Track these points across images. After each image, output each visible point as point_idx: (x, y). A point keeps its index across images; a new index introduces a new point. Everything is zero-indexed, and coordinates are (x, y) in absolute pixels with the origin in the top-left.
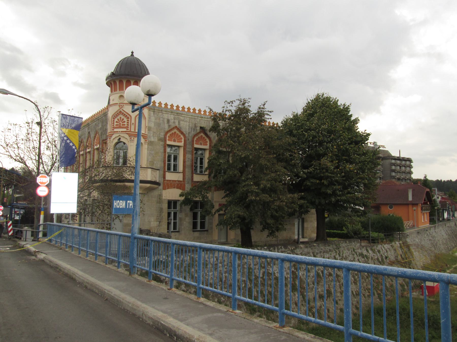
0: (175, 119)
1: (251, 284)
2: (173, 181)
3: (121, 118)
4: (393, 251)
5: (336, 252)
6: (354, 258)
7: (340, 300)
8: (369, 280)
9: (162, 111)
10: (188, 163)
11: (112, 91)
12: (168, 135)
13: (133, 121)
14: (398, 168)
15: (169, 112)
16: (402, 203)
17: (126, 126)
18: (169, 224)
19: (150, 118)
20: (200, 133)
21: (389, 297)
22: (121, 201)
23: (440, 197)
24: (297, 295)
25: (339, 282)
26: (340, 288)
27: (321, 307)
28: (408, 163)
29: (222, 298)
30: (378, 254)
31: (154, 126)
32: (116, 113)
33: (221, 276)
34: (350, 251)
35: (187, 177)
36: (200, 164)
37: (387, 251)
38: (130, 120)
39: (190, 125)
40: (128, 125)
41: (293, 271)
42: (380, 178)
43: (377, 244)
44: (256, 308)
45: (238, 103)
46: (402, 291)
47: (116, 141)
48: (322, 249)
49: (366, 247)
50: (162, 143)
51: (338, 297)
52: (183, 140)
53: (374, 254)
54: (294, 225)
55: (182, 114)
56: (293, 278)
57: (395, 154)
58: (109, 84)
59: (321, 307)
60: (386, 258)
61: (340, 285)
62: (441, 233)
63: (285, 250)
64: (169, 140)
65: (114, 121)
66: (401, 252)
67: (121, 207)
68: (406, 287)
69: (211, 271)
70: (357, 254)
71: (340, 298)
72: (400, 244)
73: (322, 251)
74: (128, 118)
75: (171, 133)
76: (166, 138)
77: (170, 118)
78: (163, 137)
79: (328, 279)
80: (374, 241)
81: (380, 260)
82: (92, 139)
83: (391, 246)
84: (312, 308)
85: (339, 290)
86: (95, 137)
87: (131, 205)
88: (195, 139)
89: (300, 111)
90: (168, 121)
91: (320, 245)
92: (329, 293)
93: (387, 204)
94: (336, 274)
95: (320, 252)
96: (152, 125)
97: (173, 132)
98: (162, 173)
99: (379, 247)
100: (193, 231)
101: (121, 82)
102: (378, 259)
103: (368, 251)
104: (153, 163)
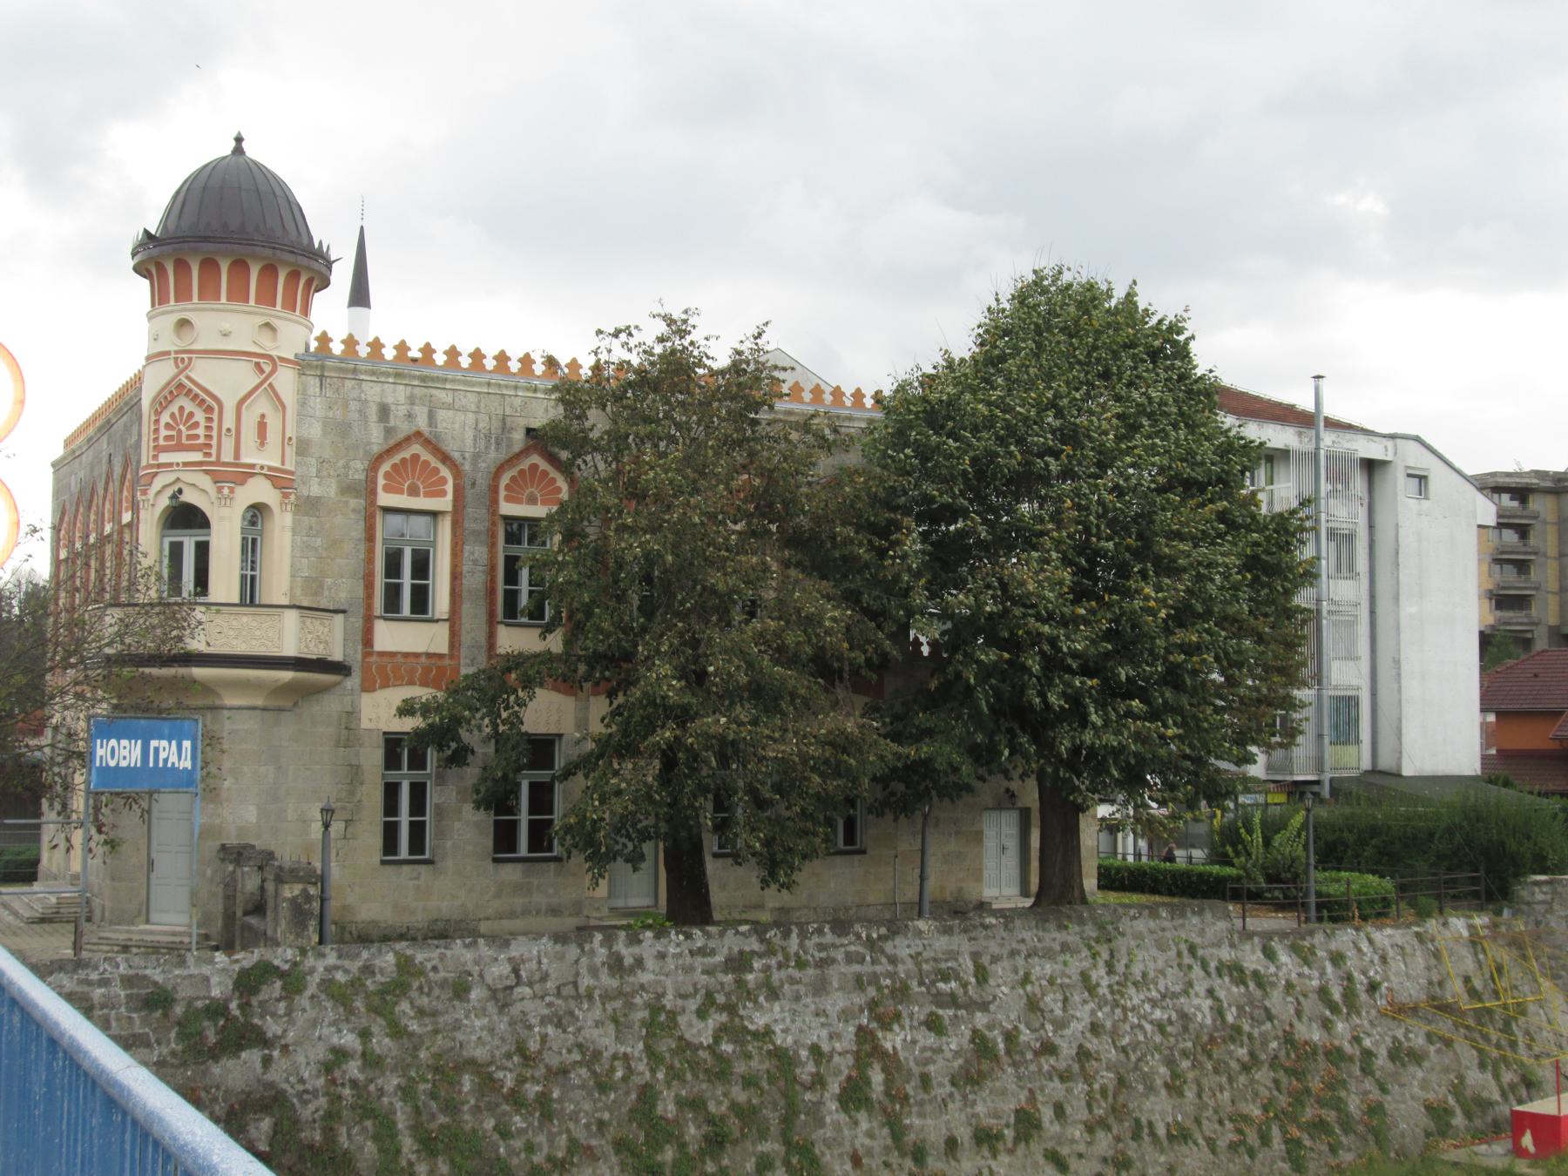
0: (412, 400)
1: (653, 1071)
2: (406, 655)
3: (182, 409)
4: (1420, 961)
5: (1094, 956)
6: (1190, 984)
7: (1080, 1156)
8: (1252, 1081)
9: (355, 371)
10: (474, 580)
11: (153, 305)
12: (386, 467)
13: (229, 422)
15: (389, 375)
17: (202, 440)
18: (390, 832)
22: (124, 742)
24: (864, 1126)
26: (1089, 1106)
29: (518, 1118)
30: (1329, 969)
31: (325, 433)
32: (166, 392)
33: (524, 1033)
34: (1172, 953)
35: (466, 639)
36: (507, 582)
37: (1384, 959)
38: (215, 416)
39: (481, 426)
41: (860, 1028)
43: (1328, 926)
44: (660, 1165)
45: (651, 333)
46: (1428, 1134)
47: (164, 502)
48: (1023, 941)
49: (1267, 936)
50: (357, 503)
51: (1073, 1141)
52: (449, 487)
53: (1306, 970)
54: (978, 837)
55: (445, 380)
56: (857, 1056)
60: (1373, 987)
63: (838, 941)
64: (387, 489)
65: (157, 421)
66: (1469, 965)
67: (124, 764)
68: (1459, 1120)
69: (483, 1012)
70: (1204, 966)
71: (1082, 1148)
72: (1471, 927)
73: (1023, 948)
74: (209, 409)
75: (396, 459)
76: (375, 482)
77: (390, 400)
78: (363, 477)
79: (1033, 1067)
80: (1333, 912)
81: (1336, 995)
82: (117, 483)
83: (1418, 935)
85: (1083, 1114)
86: (123, 476)
87: (163, 755)
88: (505, 480)
90: (384, 411)
91: (1018, 923)
92: (1027, 1124)
94: (1080, 1046)
95: (1013, 954)
97: (406, 454)
98: (358, 622)
99: (1345, 938)
100: (496, 860)
101: (182, 266)
102: (1323, 992)
103: (1269, 954)
104: (321, 586)
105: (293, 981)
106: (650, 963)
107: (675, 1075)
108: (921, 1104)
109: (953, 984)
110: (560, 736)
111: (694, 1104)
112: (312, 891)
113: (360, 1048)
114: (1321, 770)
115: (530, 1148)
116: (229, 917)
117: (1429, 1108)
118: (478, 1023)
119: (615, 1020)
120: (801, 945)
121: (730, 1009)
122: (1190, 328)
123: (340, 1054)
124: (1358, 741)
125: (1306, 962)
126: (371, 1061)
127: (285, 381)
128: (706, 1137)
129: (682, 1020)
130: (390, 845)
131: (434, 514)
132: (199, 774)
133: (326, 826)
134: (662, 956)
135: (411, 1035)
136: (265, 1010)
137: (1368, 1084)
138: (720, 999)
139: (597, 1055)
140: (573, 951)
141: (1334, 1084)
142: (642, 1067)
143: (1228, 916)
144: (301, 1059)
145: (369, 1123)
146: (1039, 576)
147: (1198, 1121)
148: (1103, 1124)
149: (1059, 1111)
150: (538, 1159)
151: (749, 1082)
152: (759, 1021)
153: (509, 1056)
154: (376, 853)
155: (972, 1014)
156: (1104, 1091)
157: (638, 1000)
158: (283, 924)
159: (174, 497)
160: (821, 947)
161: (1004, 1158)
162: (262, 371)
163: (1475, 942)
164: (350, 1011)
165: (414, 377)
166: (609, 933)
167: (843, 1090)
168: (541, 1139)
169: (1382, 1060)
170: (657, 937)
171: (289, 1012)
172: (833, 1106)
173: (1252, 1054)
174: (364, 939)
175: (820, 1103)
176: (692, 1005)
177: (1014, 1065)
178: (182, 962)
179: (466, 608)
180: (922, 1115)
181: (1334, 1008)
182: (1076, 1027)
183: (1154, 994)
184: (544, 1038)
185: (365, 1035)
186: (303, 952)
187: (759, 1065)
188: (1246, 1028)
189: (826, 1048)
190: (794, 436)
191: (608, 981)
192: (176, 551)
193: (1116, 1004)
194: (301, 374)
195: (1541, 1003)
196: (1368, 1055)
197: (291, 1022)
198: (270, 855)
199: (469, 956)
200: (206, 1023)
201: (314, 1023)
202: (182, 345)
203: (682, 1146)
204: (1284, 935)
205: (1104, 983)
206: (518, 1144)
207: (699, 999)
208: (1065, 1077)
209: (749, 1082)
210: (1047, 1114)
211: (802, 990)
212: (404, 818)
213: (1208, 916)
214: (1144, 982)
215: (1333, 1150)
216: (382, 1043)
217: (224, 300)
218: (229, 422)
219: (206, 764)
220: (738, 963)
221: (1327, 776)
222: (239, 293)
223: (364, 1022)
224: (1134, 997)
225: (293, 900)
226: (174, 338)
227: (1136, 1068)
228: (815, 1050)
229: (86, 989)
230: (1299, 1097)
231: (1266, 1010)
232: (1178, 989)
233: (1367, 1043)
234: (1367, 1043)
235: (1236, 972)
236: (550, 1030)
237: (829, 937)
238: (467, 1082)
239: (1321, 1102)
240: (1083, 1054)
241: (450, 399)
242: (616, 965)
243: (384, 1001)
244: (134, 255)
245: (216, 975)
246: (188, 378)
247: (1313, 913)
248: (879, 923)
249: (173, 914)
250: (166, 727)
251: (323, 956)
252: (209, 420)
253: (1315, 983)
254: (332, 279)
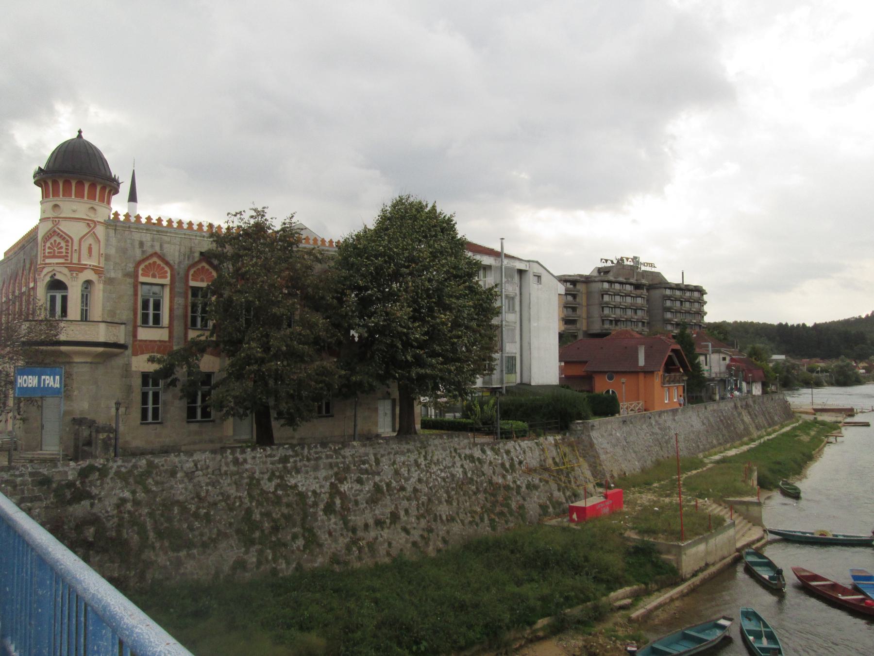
0: (153, 240)
1: (251, 503)
2: (151, 341)
5: (420, 453)
6: (455, 463)
7: (414, 528)
8: (477, 498)
10: (179, 312)
12: (142, 266)
13: (76, 247)
14: (678, 304)
15: (142, 229)
16: (628, 370)
17: (64, 254)
20: (199, 261)
21: (512, 525)
22: (30, 377)
23: (728, 358)
24: (333, 520)
25: (417, 500)
26: (418, 510)
27: (376, 538)
28: (696, 294)
30: (505, 456)
34: (448, 452)
35: (175, 334)
37: (524, 452)
39: (182, 250)
41: (332, 484)
42: (643, 323)
46: (540, 515)
47: (48, 279)
49: (483, 445)
50: (131, 281)
52: (169, 275)
54: (376, 410)
56: (330, 494)
57: (673, 278)
59: (376, 538)
60: (520, 463)
61: (418, 505)
62: (693, 421)
64: (143, 275)
66: (554, 453)
67: (30, 386)
68: (551, 510)
69: (182, 482)
70: (460, 456)
71: (415, 525)
72: (555, 440)
74: (67, 241)
77: (144, 240)
80: (507, 435)
81: (508, 466)
84: (359, 539)
85: (416, 513)
86: (30, 268)
87: (47, 382)
88: (192, 272)
89: (372, 226)
90: (141, 244)
92: (395, 517)
93: (605, 372)
95: (389, 453)
96: (112, 251)
97: (151, 261)
98: (130, 328)
99: (510, 445)
100: (188, 422)
101: (55, 183)
102: (503, 465)
103: (484, 451)
104: (115, 313)
105: (103, 472)
106: (249, 461)
107: (259, 504)
108: (355, 511)
109: (367, 466)
110: (213, 373)
111: (268, 514)
112: (111, 435)
113: (131, 498)
114: (502, 382)
115: (202, 535)
116: (76, 447)
117: (540, 506)
118: (180, 486)
119: (236, 483)
120: (309, 452)
121: (281, 477)
122: (455, 219)
123: (124, 501)
124: (516, 373)
125: (497, 454)
126: (136, 503)
127: (100, 231)
128: (272, 528)
129: (262, 482)
130: (144, 416)
131: (163, 286)
132: (63, 390)
133: (117, 409)
134: (254, 458)
135: (153, 491)
136: (92, 483)
137: (519, 498)
138: (277, 474)
139: (229, 497)
140: (219, 457)
141: (507, 498)
142: (247, 501)
143: (468, 438)
144: (107, 503)
145: (136, 528)
146: (401, 311)
147: (458, 514)
148: (423, 516)
149: (407, 511)
150: (205, 539)
151: (288, 505)
152: (293, 481)
153: (193, 499)
154: (139, 421)
155: (374, 476)
156: (423, 504)
157: (245, 475)
158: (99, 449)
159: (52, 277)
160: (316, 453)
161: (386, 531)
163: (556, 445)
164: (127, 483)
166: (233, 450)
167: (325, 507)
168: (206, 530)
169: (524, 489)
170: (252, 450)
171: (102, 484)
172: (321, 513)
173: (477, 488)
174: (134, 454)
175: (315, 513)
176: (266, 476)
177: (390, 495)
178: (56, 466)
179: (176, 323)
180: (355, 516)
181: (507, 471)
182: (413, 480)
183: (442, 467)
184: (207, 491)
185: (134, 492)
186: (108, 460)
187: (292, 498)
188: (475, 479)
189: (318, 491)
190: (306, 257)
191: (233, 468)
192: (53, 299)
193: (428, 471)
194: (107, 228)
195: (579, 467)
196: (519, 487)
197: (103, 489)
198: (94, 422)
199: (177, 460)
200: (66, 490)
201: (112, 489)
202: (55, 215)
203: (263, 531)
204: (488, 444)
205: (423, 463)
206: (197, 533)
207: (269, 474)
208: (409, 499)
209: (288, 505)
210: (402, 513)
211: (309, 469)
212: (150, 406)
213: (461, 438)
214: (438, 463)
215: (507, 522)
216: (141, 495)
218: (76, 247)
219: (65, 386)
220: (284, 460)
221: (504, 386)
222: (80, 194)
223: (133, 488)
224: (434, 468)
225: (103, 440)
227: (435, 495)
228: (314, 492)
229: (13, 478)
230: (494, 504)
231: (482, 472)
232: (450, 465)
233: (518, 483)
234: (518, 483)
235: (471, 458)
236: (210, 488)
237: (319, 449)
238: (176, 510)
239: (502, 505)
240: (415, 490)
242: (236, 462)
243: (141, 480)
244: (34, 177)
245: (71, 471)
247: (499, 436)
248: (338, 443)
249: (52, 447)
250: (48, 370)
251: (116, 461)
253: (500, 461)
254: (120, 190)
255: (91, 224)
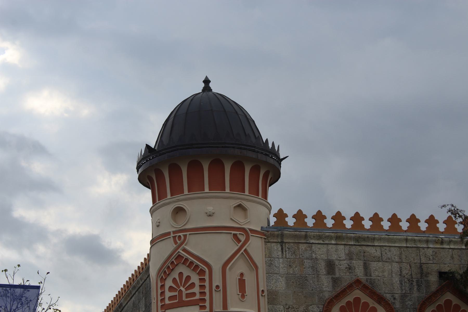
0: (350, 256)
3: (181, 274)
9: (306, 237)
11: (154, 201)
13: (217, 281)
15: (330, 238)
17: (198, 297)
19: (270, 264)
20: (440, 292)
32: (168, 264)
38: (207, 277)
39: (404, 272)
40: (203, 293)
55: (374, 239)
58: (145, 179)
65: (163, 286)
74: (202, 272)
75: (343, 302)
77: (334, 257)
90: (331, 266)
97: (350, 298)
127: (256, 247)
162: (239, 241)
165: (350, 238)
217: (207, 190)
218: (217, 281)
222: (217, 184)
226: (172, 222)
241: (378, 254)
244: (138, 168)
246: (184, 250)
252: (202, 280)
255: (240, 234)
